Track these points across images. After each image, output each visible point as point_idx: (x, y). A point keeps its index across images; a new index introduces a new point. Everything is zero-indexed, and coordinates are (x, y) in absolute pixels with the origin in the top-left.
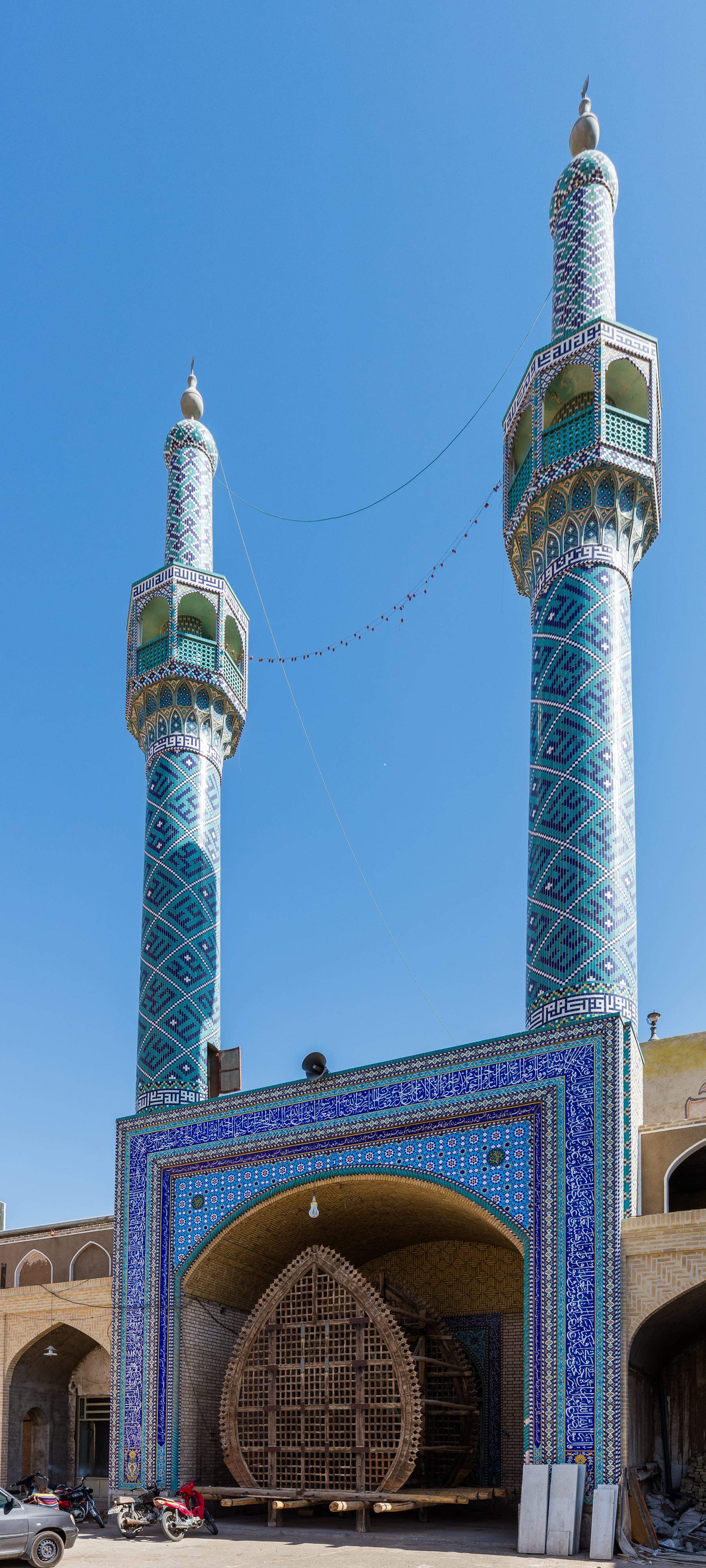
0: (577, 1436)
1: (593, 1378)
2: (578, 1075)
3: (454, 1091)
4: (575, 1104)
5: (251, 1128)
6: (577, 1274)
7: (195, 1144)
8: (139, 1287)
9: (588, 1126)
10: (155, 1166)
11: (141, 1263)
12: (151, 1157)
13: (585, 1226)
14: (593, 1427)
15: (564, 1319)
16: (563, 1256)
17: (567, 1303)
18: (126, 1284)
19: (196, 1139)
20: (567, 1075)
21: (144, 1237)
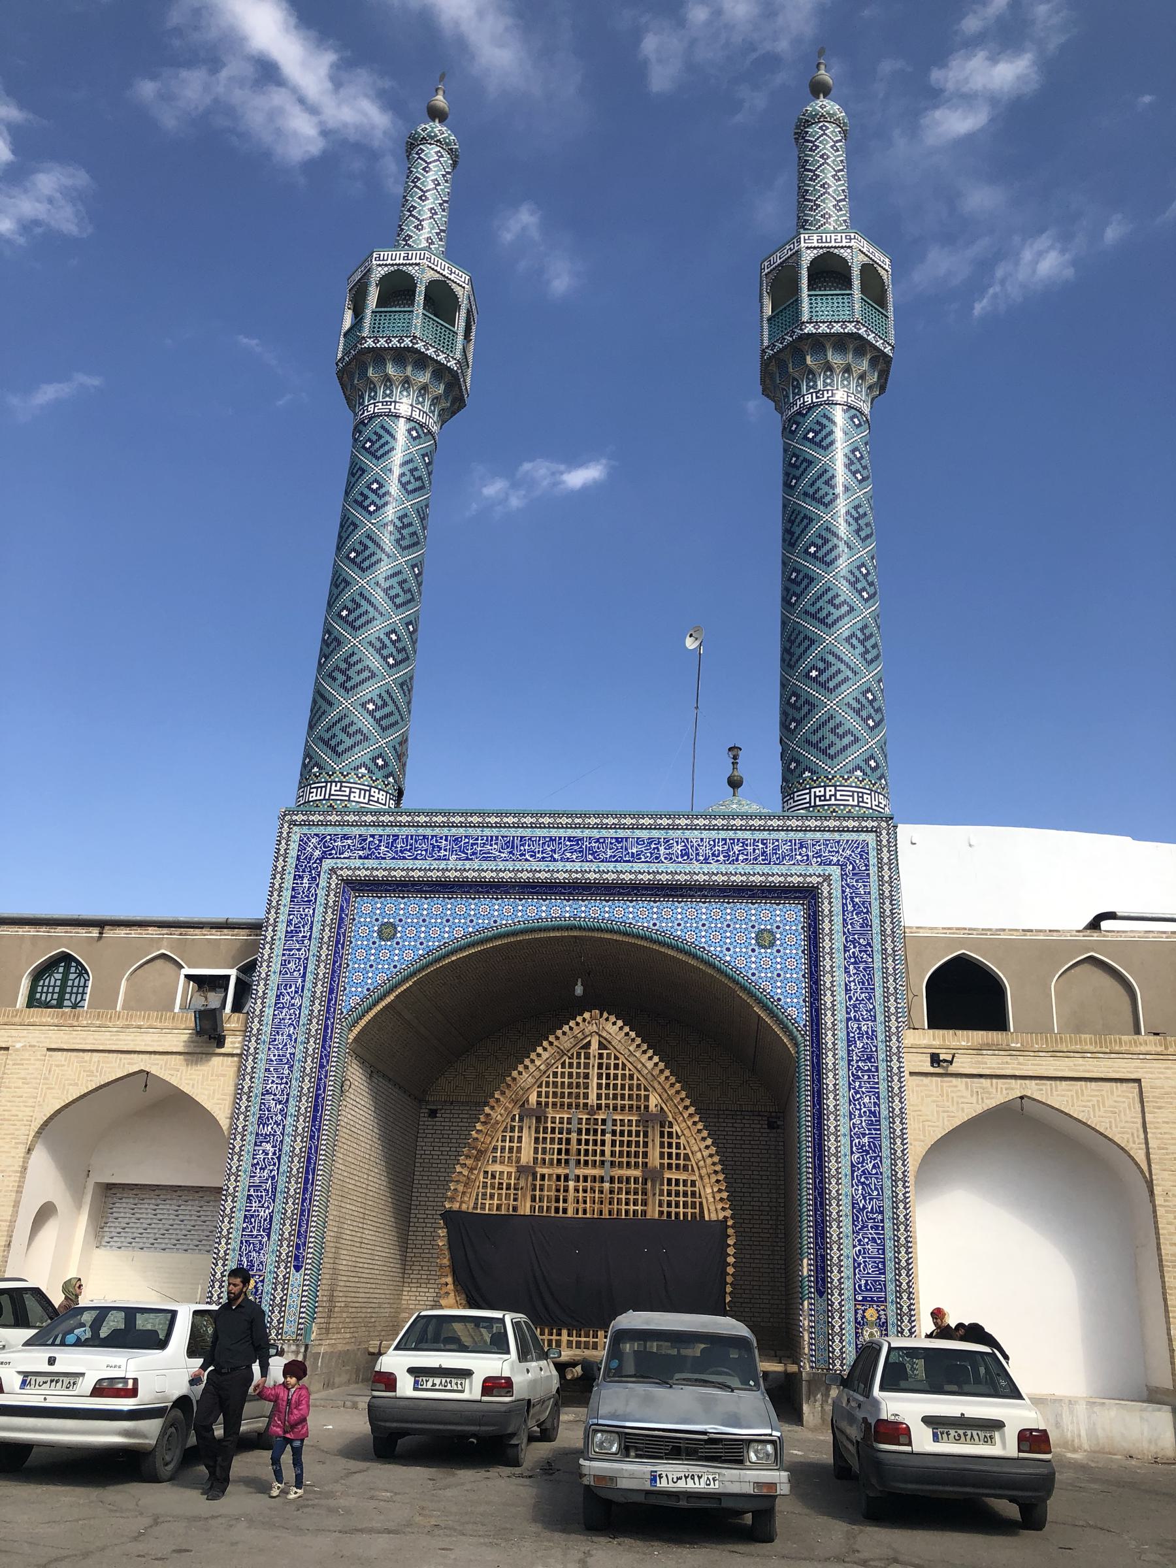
0: (867, 1284)
1: (882, 1213)
2: (854, 869)
3: (721, 858)
4: (852, 898)
5: (473, 854)
6: (860, 1087)
7: (394, 858)
8: (289, 1035)
9: (866, 924)
10: (334, 877)
11: (297, 1001)
12: (328, 864)
13: (867, 1033)
14: (884, 1273)
15: (848, 1138)
16: (844, 1064)
17: (851, 1119)
18: (267, 1029)
19: (396, 852)
20: (843, 866)
21: (305, 968)
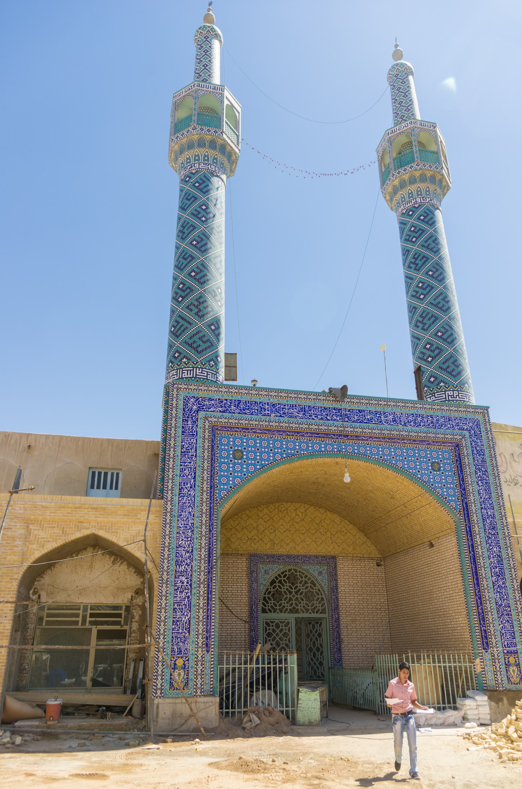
0: (508, 644)
1: (509, 607)
2: (475, 433)
3: (412, 423)
4: (475, 447)
5: (284, 413)
6: (492, 543)
7: (239, 413)
8: (189, 512)
9: (483, 461)
10: (207, 422)
11: (192, 493)
12: (201, 414)
13: (491, 515)
14: (515, 638)
15: (489, 569)
16: (483, 530)
17: (489, 559)
18: (176, 508)
19: (241, 410)
20: (470, 431)
21: (195, 473)
